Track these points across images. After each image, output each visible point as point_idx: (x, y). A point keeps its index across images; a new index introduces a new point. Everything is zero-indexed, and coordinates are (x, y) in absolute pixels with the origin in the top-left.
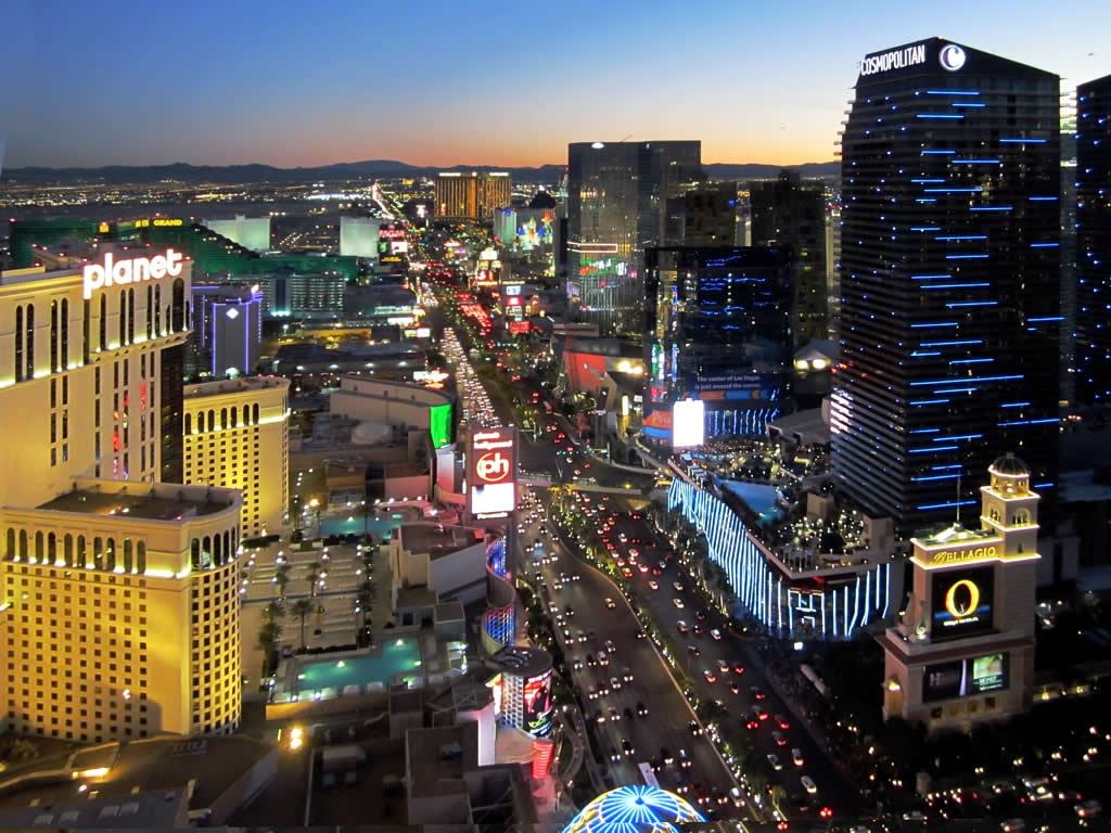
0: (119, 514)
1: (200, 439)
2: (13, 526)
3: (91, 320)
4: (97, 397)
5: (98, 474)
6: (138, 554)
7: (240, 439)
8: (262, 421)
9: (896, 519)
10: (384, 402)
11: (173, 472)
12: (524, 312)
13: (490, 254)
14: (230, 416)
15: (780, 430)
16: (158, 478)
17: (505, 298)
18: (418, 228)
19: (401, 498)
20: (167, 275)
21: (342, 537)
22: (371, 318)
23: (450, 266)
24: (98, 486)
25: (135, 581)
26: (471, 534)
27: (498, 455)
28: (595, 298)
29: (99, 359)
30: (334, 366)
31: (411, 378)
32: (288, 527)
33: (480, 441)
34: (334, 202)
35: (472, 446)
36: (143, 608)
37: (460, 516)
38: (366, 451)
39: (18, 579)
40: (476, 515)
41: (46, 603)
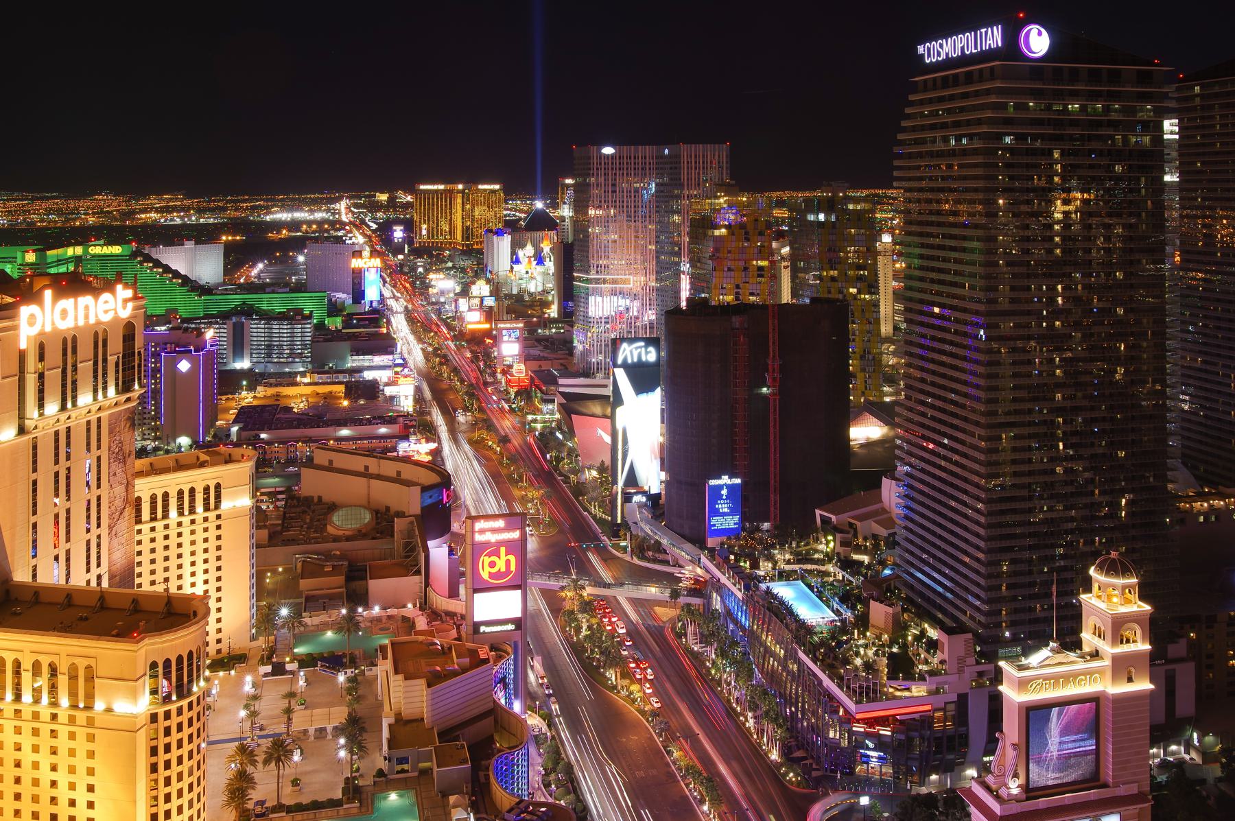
4: (34, 476)
5: (34, 576)
7: (199, 528)
8: (226, 505)
9: (976, 634)
13: (481, 288)
14: (186, 501)
15: (834, 518)
18: (395, 255)
23: (434, 304)
27: (503, 550)
29: (36, 427)
32: (255, 644)
33: (482, 531)
34: (295, 225)
37: (458, 627)
40: (476, 626)
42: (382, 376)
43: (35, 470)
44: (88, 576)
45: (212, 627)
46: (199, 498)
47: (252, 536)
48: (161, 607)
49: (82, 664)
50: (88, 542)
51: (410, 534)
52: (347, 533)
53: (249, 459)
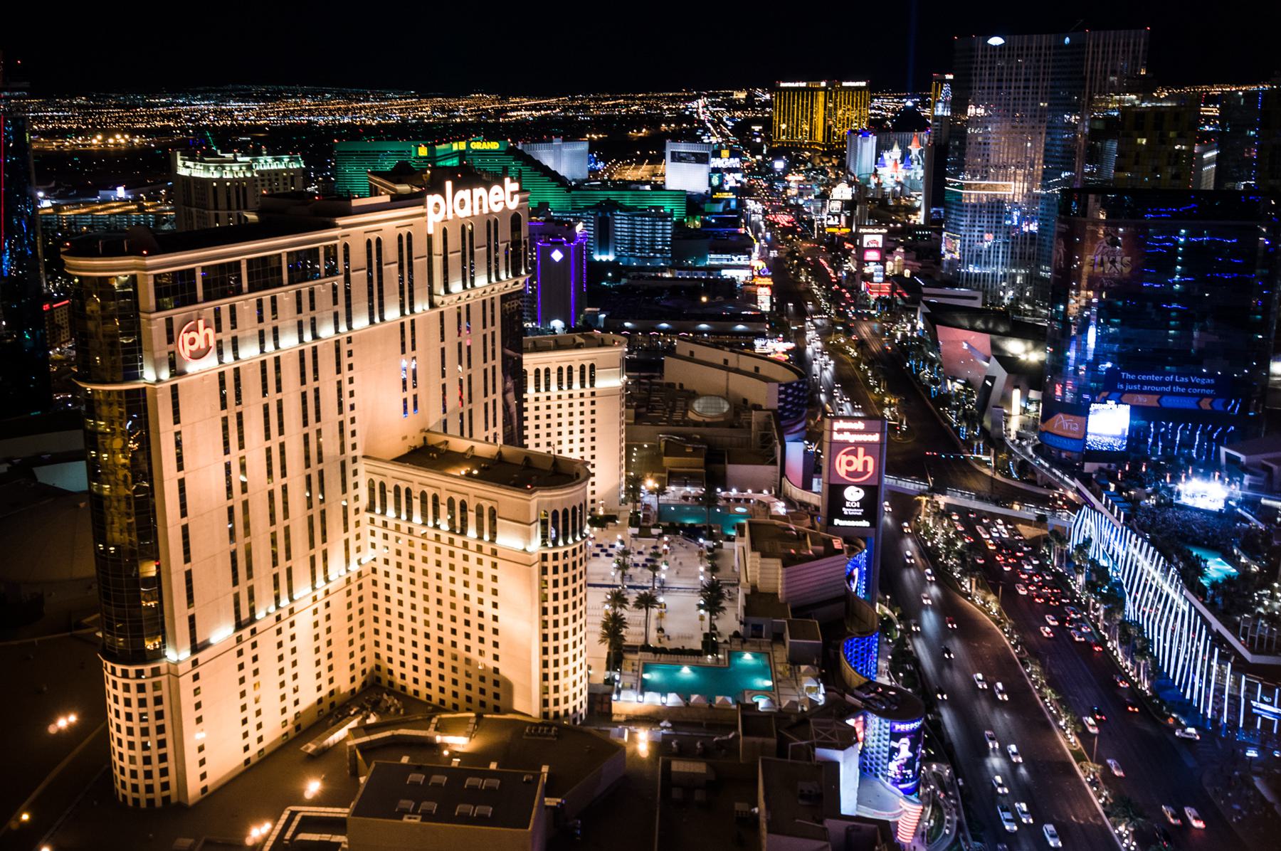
0: (469, 476)
1: (537, 399)
2: (374, 477)
3: (435, 258)
4: (443, 345)
6: (491, 519)
7: (576, 402)
8: (598, 384)
10: (724, 372)
11: (514, 433)
12: (884, 271)
14: (566, 376)
16: (500, 441)
17: (861, 250)
19: (748, 492)
20: (505, 208)
21: (682, 526)
22: (701, 269)
24: (447, 442)
25: (487, 548)
26: (828, 543)
28: (979, 256)
30: (665, 325)
31: (752, 347)
32: (623, 507)
35: (831, 436)
36: (495, 578)
38: (706, 431)
39: (380, 532)
41: (404, 559)
42: (741, 276)
43: (443, 340)
44: (486, 434)
45: (590, 488)
46: (576, 375)
47: (621, 414)
48: (548, 466)
49: (487, 505)
50: (486, 405)
51: (766, 426)
52: (707, 420)
53: (620, 344)
